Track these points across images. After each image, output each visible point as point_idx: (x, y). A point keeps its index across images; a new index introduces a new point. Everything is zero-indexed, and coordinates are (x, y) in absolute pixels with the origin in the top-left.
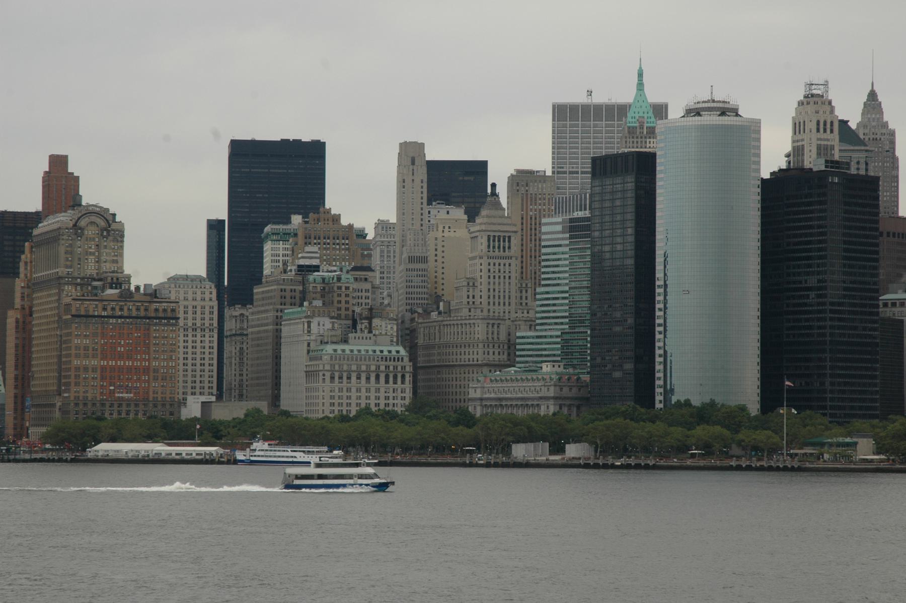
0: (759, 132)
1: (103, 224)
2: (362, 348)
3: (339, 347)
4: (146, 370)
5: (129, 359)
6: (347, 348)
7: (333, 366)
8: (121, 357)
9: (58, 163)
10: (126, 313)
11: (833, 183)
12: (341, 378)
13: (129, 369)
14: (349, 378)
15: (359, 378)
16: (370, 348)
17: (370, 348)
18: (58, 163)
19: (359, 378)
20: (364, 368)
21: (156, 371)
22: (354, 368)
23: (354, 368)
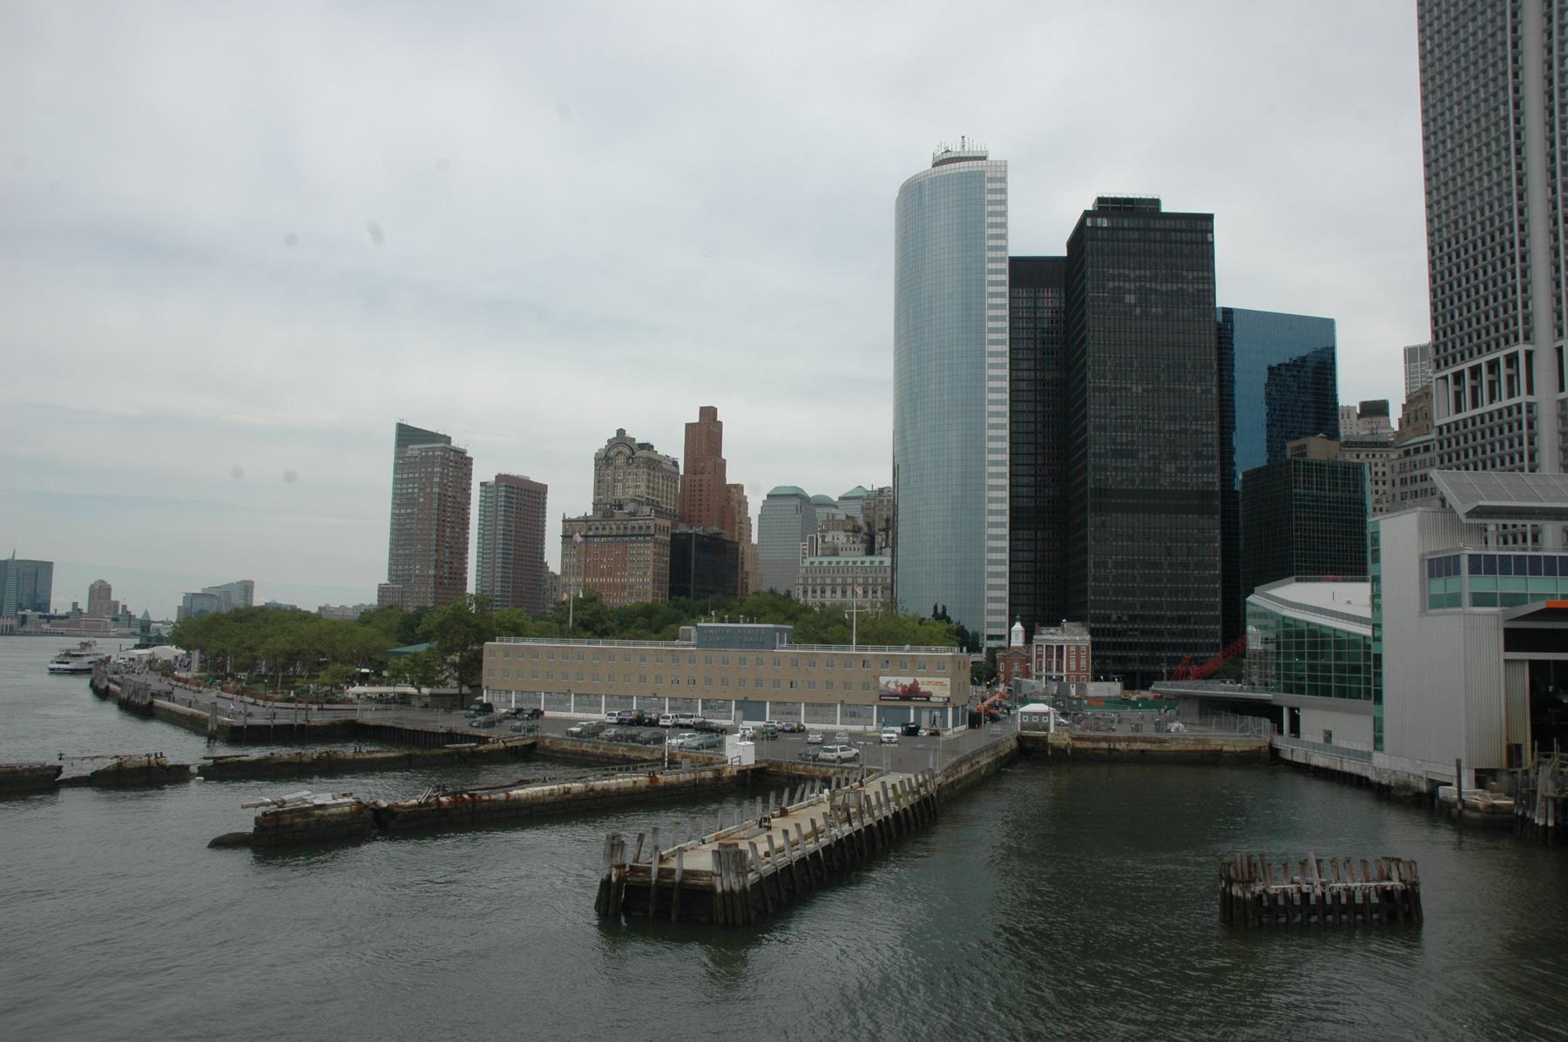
0: (1003, 180)
1: (628, 452)
2: (851, 560)
3: (826, 560)
4: (624, 587)
5: (610, 575)
6: (834, 559)
7: (805, 579)
8: (602, 575)
9: (709, 414)
10: (607, 532)
11: (1095, 228)
12: (814, 592)
13: (609, 585)
14: (823, 592)
15: (834, 592)
16: (851, 560)
17: (859, 559)
18: (709, 414)
19: (834, 592)
20: (849, 580)
21: (632, 587)
22: (828, 581)
23: (828, 581)
